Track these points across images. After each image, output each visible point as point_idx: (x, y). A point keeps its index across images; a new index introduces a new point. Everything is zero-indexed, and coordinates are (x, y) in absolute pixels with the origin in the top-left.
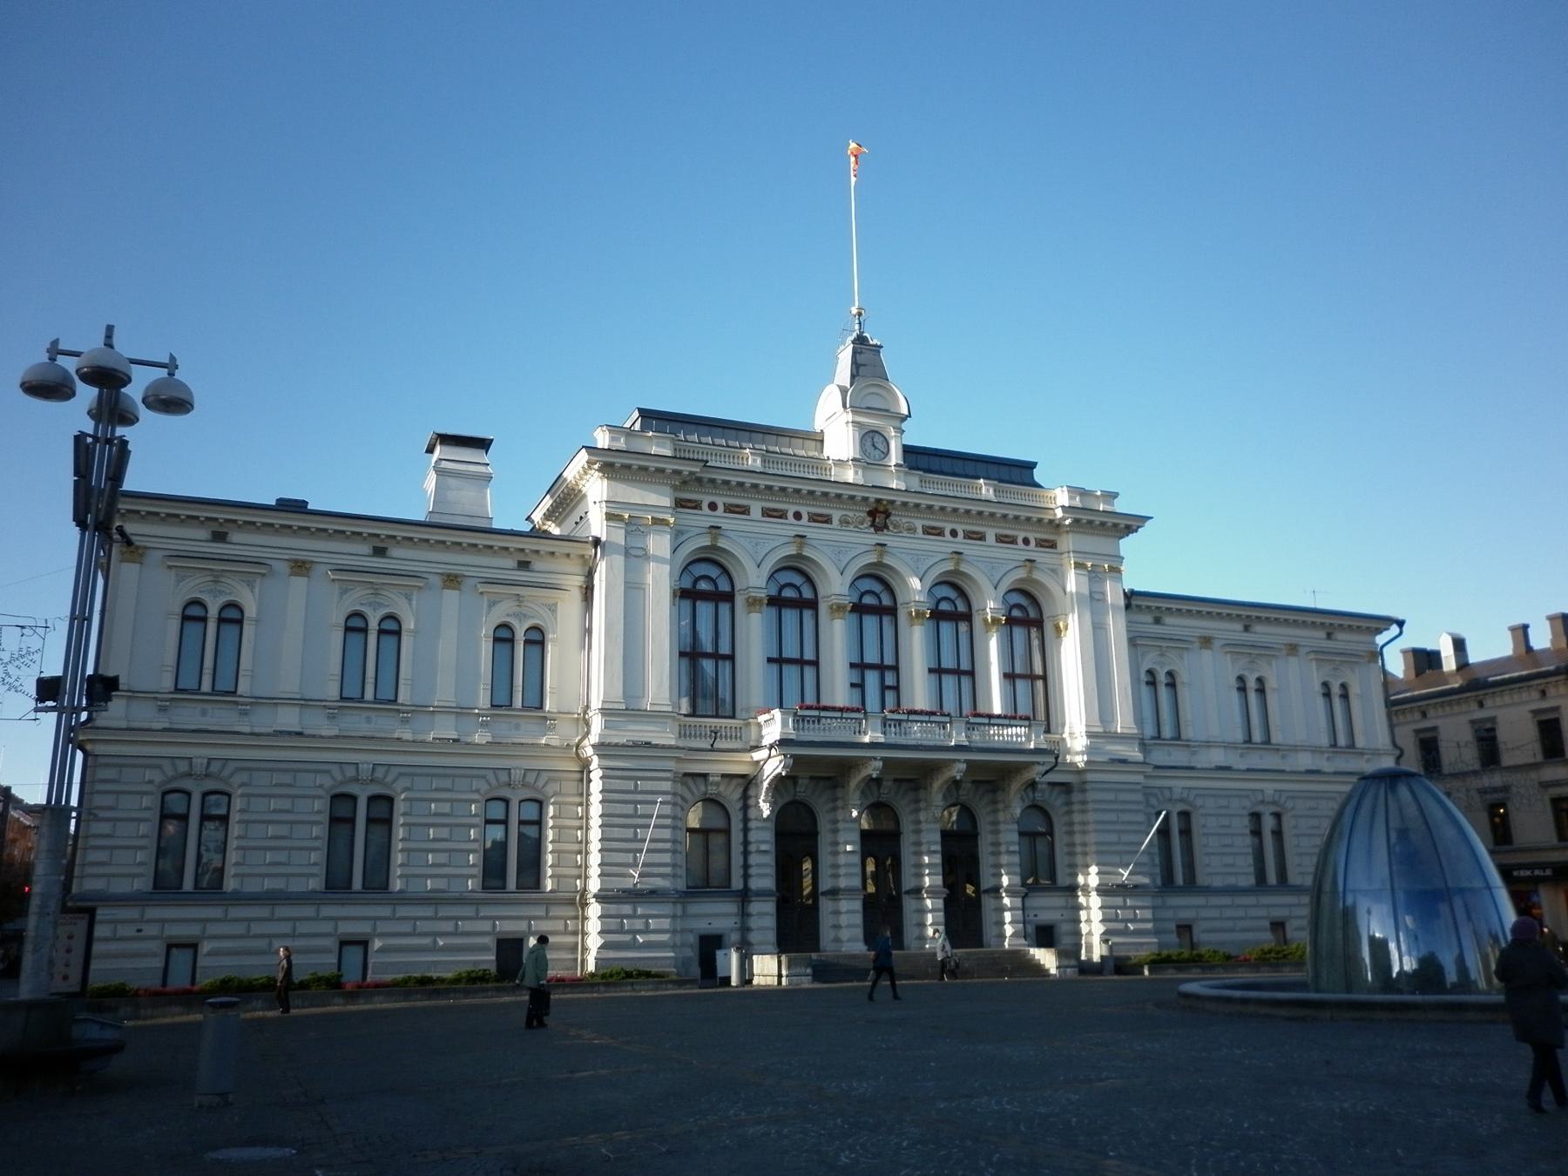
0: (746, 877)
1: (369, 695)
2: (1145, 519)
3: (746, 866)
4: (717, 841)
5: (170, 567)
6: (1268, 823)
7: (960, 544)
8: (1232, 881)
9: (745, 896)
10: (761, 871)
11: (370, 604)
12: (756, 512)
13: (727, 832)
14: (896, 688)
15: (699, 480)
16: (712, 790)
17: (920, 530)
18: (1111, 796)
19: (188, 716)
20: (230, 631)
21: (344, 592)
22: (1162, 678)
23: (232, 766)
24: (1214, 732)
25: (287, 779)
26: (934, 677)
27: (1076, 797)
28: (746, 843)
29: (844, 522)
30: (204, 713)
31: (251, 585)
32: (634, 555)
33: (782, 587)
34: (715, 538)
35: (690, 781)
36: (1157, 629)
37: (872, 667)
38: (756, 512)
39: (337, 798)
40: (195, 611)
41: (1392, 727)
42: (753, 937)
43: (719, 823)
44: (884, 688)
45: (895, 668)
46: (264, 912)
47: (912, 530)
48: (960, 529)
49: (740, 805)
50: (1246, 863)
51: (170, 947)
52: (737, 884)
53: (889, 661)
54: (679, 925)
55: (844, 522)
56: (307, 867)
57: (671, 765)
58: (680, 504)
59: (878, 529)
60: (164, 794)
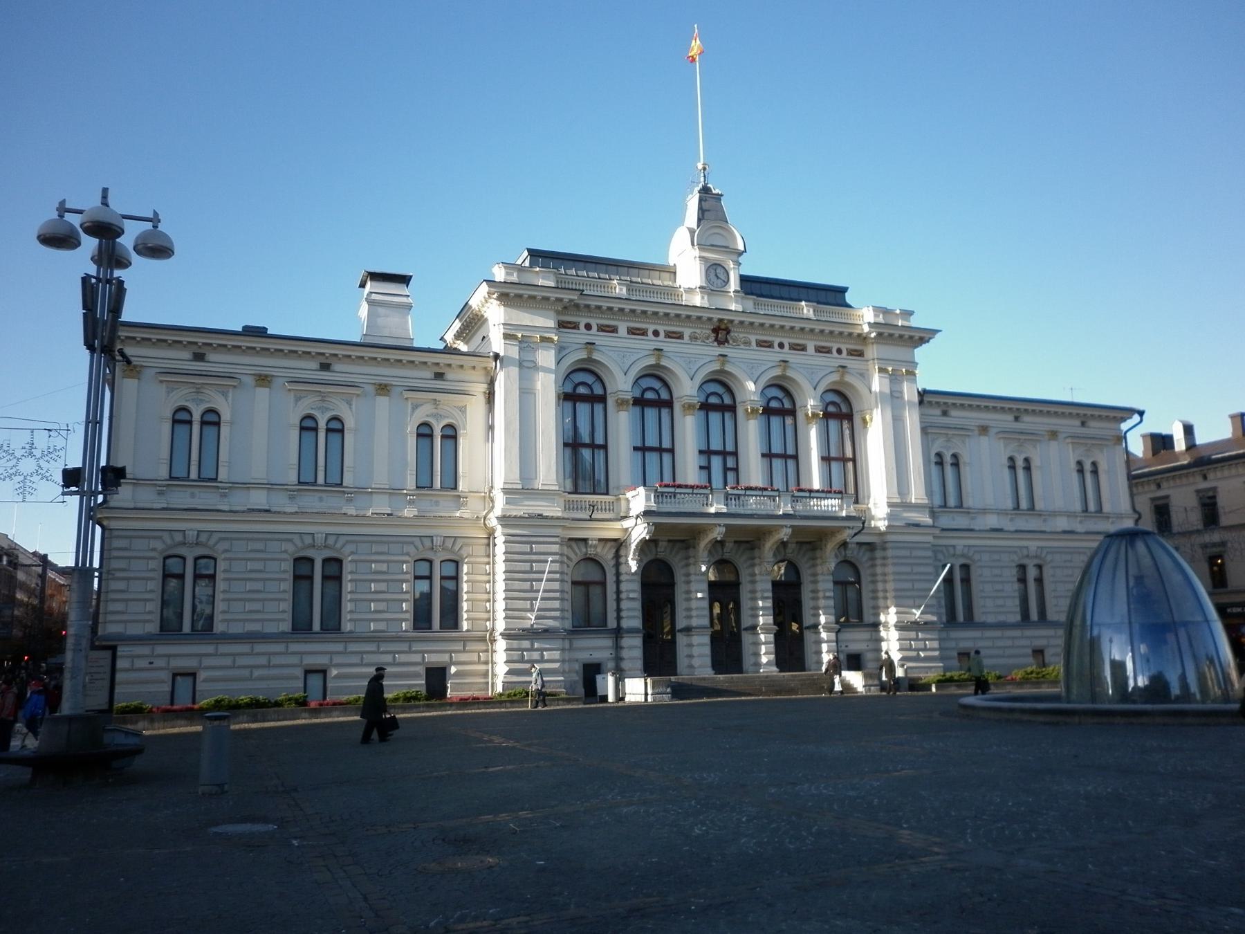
0: (619, 618)
1: (321, 480)
2: (934, 332)
3: (619, 610)
4: (595, 591)
5: (161, 382)
6: (1032, 573)
7: (786, 354)
8: (1002, 618)
9: (618, 633)
10: (631, 614)
11: (319, 408)
12: (623, 331)
13: (603, 584)
14: (736, 470)
15: (577, 306)
16: (591, 551)
17: (754, 343)
19: (181, 498)
20: (210, 431)
21: (298, 399)
22: (948, 459)
23: (215, 537)
24: (990, 501)
25: (259, 546)
26: (766, 460)
27: (879, 554)
28: (618, 592)
29: (694, 338)
31: (225, 394)
32: (526, 367)
33: (644, 391)
34: (590, 352)
35: (574, 544)
36: (945, 420)
37: (716, 453)
38: (623, 331)
39: (298, 560)
40: (183, 416)
41: (1132, 495)
42: (625, 665)
43: (595, 576)
44: (726, 469)
45: (735, 454)
46: (245, 648)
47: (748, 343)
48: (786, 342)
49: (613, 562)
50: (1014, 604)
51: (175, 675)
52: (612, 624)
53: (730, 448)
54: (567, 657)
55: (694, 338)
56: (278, 614)
57: (559, 531)
58: (562, 325)
59: (721, 342)
60: (165, 558)
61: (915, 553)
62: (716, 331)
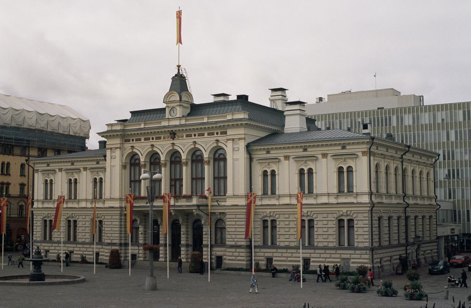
17: (185, 136)
18: (234, 216)
23: (313, 212)
29: (164, 138)
30: (48, 204)
31: (53, 175)
55: (164, 138)
59: (173, 138)
61: (238, 216)
62: (170, 134)
